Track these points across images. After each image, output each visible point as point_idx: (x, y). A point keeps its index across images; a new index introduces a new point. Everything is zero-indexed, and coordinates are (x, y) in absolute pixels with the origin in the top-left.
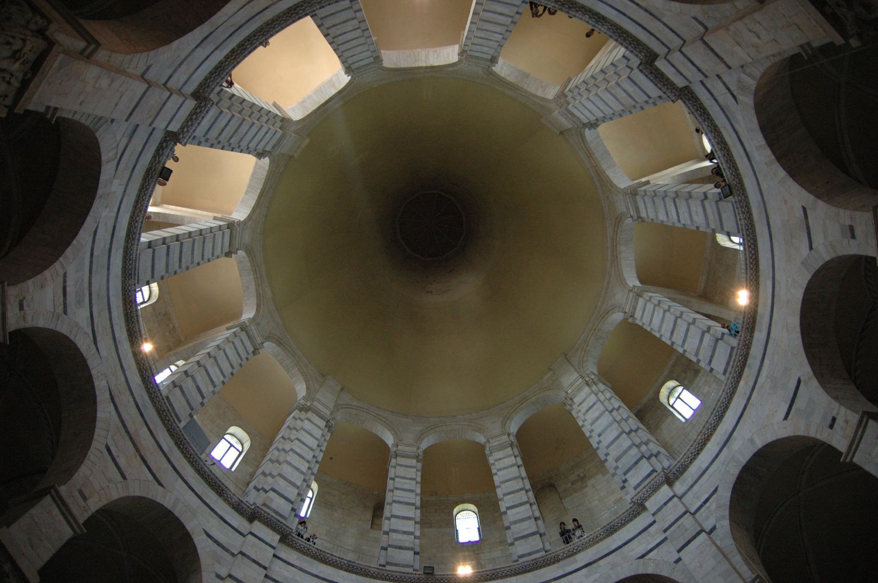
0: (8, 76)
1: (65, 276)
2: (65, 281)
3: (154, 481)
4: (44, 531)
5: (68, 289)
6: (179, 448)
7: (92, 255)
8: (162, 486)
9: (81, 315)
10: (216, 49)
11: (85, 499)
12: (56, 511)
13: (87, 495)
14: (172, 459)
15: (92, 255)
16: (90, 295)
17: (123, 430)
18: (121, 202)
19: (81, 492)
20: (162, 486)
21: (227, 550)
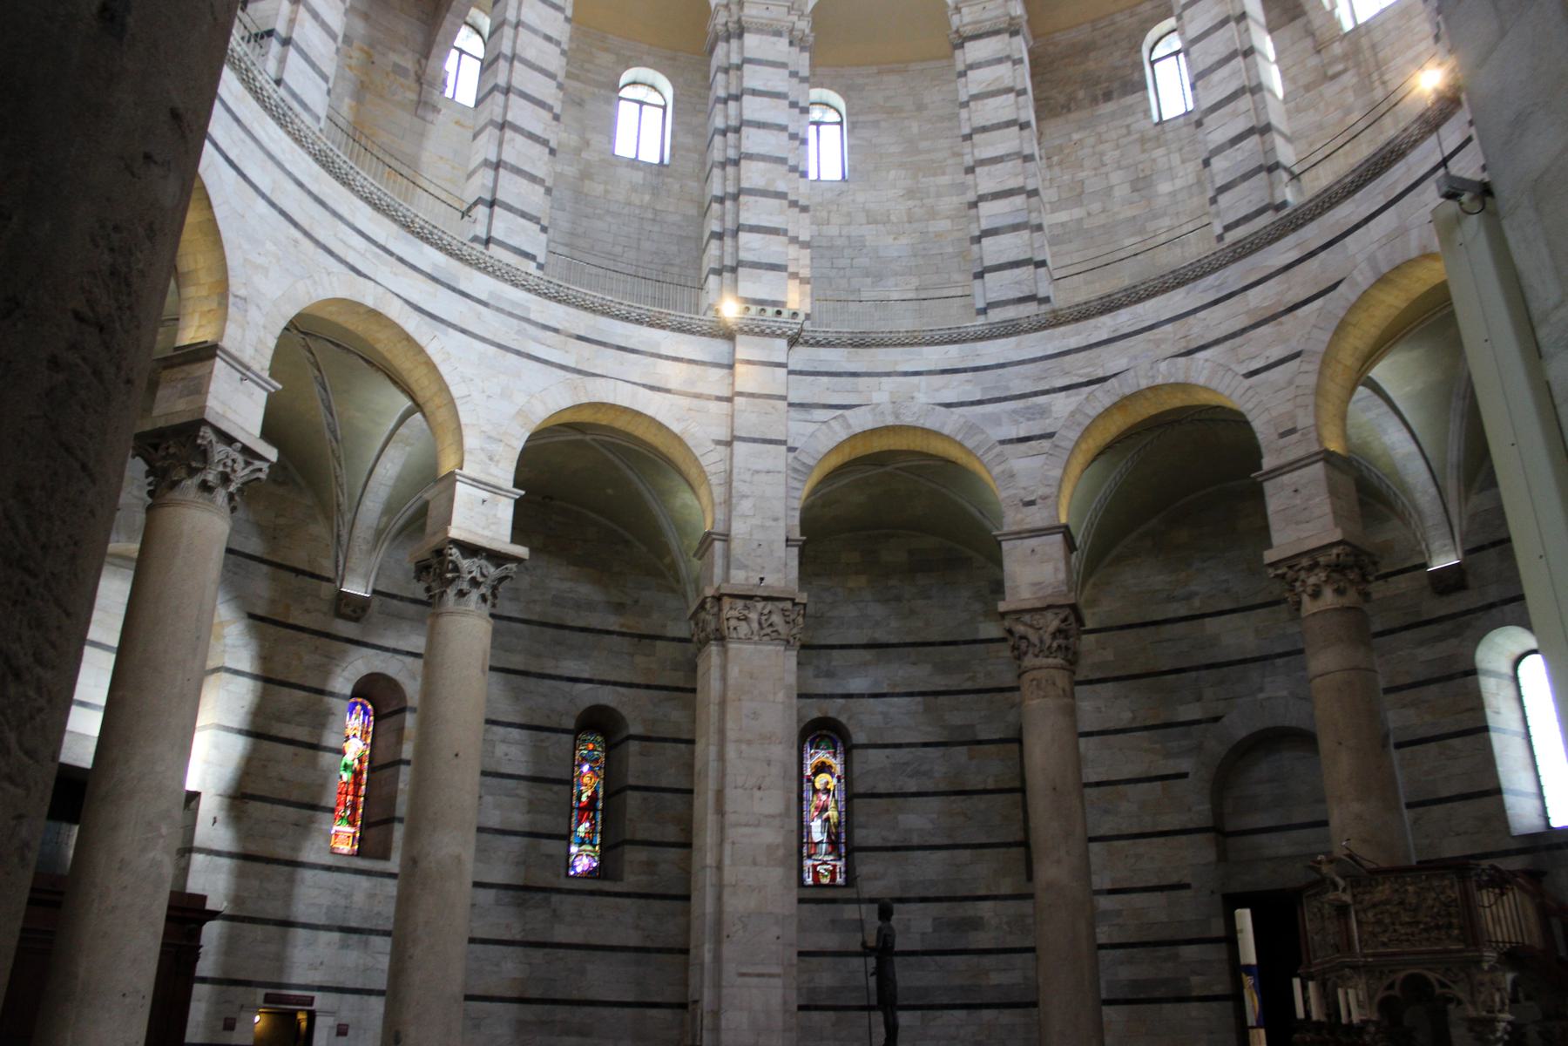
1: (1003, 442)
2: (1011, 441)
3: (1328, 296)
5: (1022, 434)
6: (1302, 225)
7: (980, 402)
8: (1340, 282)
9: (1062, 405)
10: (660, 356)
11: (1292, 431)
12: (1286, 478)
13: (1290, 426)
14: (1313, 247)
15: (980, 402)
16: (1036, 394)
17: (1238, 340)
18: (906, 374)
20: (1340, 282)
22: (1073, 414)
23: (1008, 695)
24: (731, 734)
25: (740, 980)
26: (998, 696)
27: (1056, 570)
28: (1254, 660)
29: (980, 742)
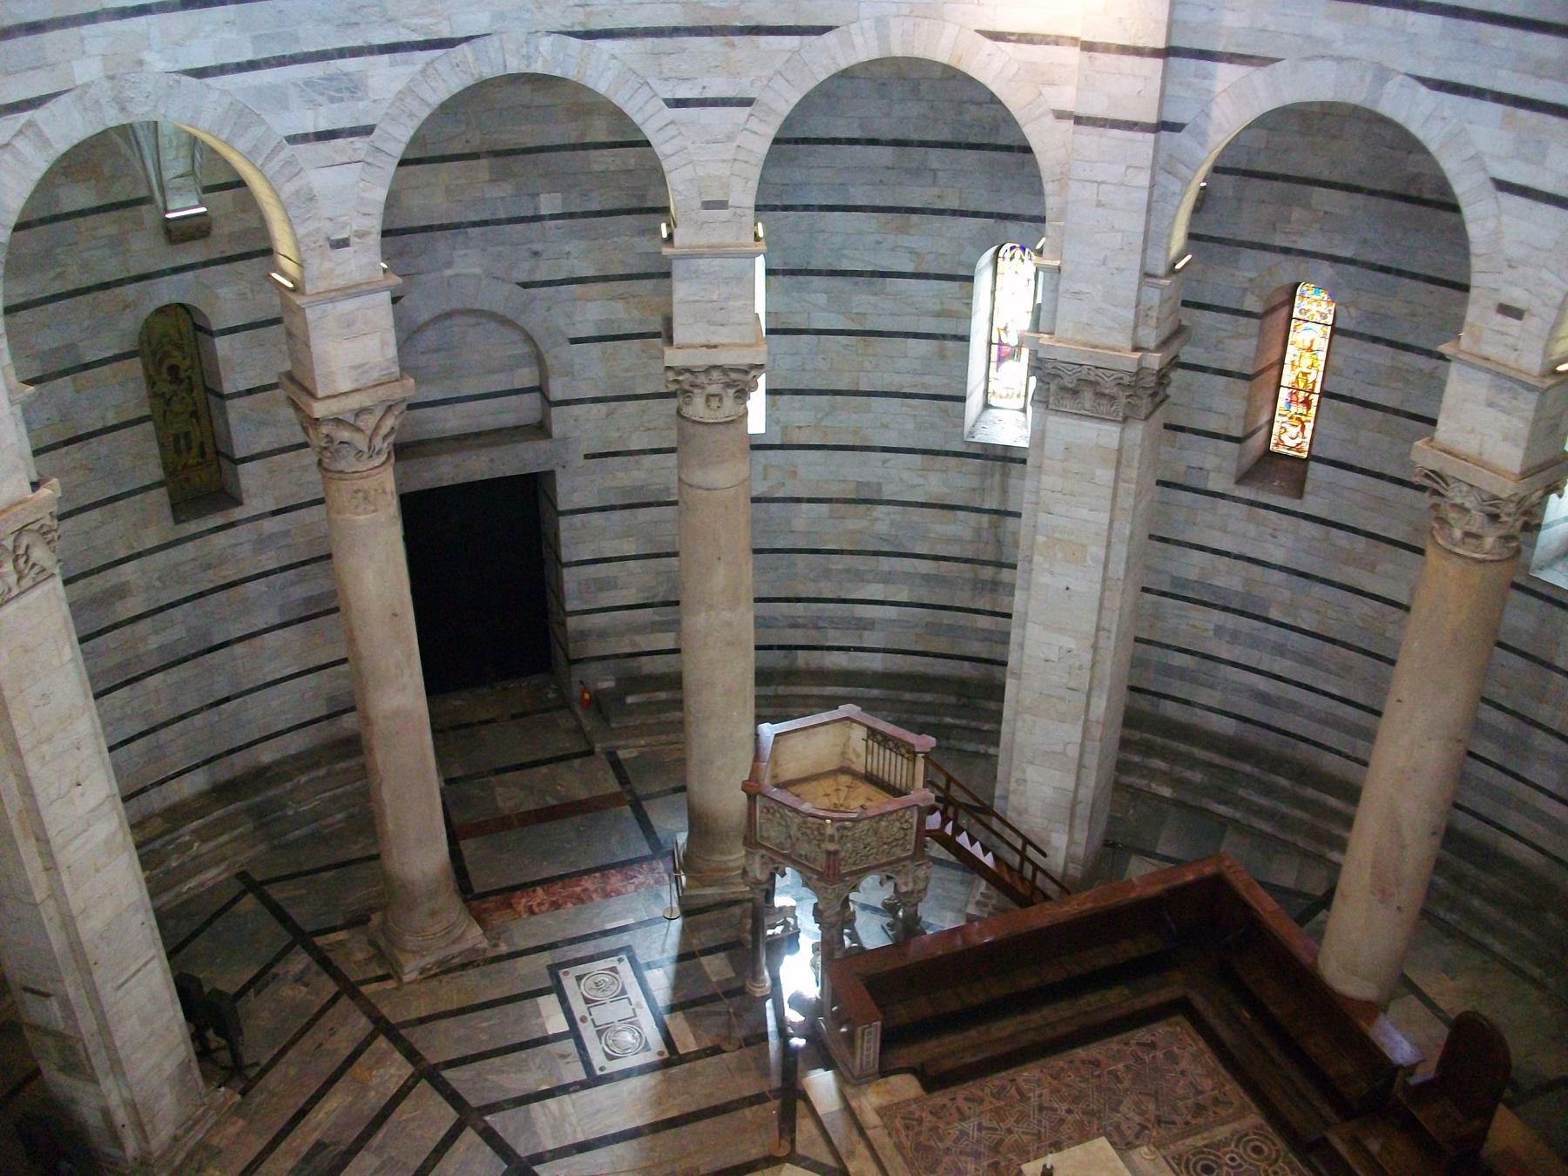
0: (22, 561)
1: (293, 139)
2: (304, 138)
3: (807, 39)
4: (715, 297)
5: (323, 126)
7: (252, 65)
11: (723, 205)
13: (717, 196)
15: (252, 65)
16: (342, 53)
19: (708, 205)
21: (1057, 41)
22: (400, 96)
23: (117, 291)
24: (25, 745)
25: (120, 993)
26: (101, 295)
27: (384, 344)
28: (442, 227)
29: (87, 366)
